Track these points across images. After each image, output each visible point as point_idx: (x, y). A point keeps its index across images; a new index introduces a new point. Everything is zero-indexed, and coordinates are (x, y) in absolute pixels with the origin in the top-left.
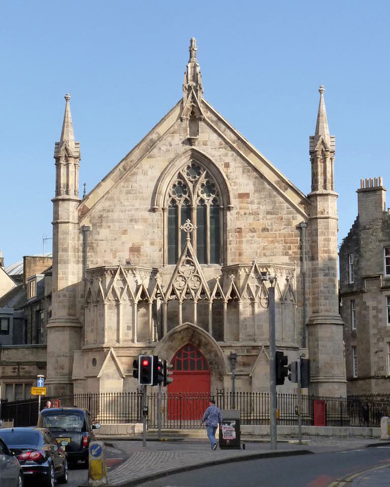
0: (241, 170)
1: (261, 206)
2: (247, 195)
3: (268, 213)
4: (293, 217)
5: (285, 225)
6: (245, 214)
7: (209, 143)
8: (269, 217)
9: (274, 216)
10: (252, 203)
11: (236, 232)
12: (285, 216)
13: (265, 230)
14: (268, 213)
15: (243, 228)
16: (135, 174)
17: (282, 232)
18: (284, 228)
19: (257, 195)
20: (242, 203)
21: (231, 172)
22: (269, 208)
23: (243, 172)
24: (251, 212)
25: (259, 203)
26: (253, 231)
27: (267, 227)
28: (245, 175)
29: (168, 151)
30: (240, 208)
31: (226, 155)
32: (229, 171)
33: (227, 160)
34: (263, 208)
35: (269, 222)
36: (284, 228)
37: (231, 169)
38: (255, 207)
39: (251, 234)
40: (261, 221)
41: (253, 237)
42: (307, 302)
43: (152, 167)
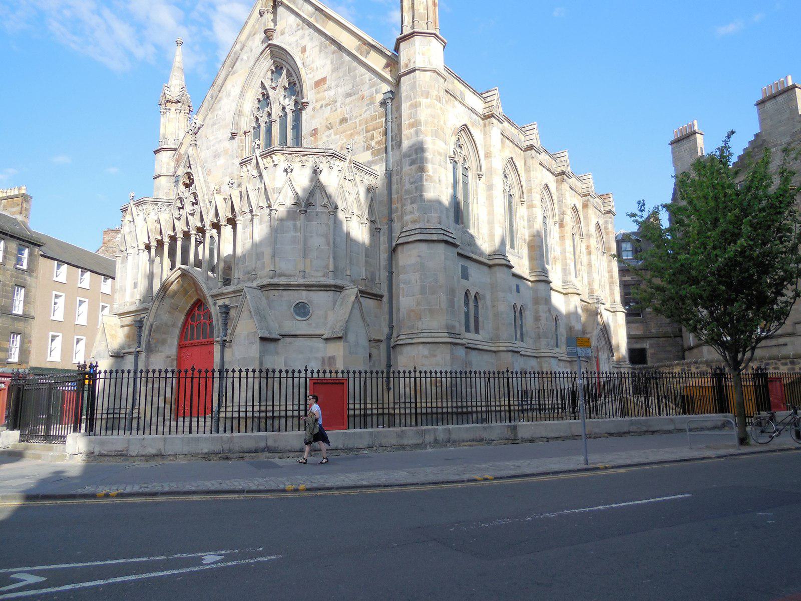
0: (318, 48)
1: (339, 89)
2: (324, 80)
3: (348, 95)
4: (376, 91)
5: (368, 105)
6: (322, 107)
7: (287, 30)
8: (348, 100)
9: (353, 98)
10: (329, 88)
11: (311, 136)
12: (367, 93)
13: (344, 120)
14: (348, 95)
15: (319, 127)
16: (221, 99)
17: (364, 116)
18: (366, 111)
19: (334, 75)
20: (318, 93)
21: (307, 58)
22: (347, 88)
23: (321, 51)
24: (328, 102)
25: (337, 86)
26: (329, 127)
27: (346, 116)
28: (322, 54)
29: (249, 58)
30: (317, 101)
31: (303, 37)
32: (306, 56)
33: (304, 42)
34: (341, 90)
35: (348, 108)
36: (366, 111)
37: (307, 53)
38: (331, 93)
39: (327, 133)
40: (339, 110)
41: (329, 136)
42: (394, 216)
43: (234, 85)
